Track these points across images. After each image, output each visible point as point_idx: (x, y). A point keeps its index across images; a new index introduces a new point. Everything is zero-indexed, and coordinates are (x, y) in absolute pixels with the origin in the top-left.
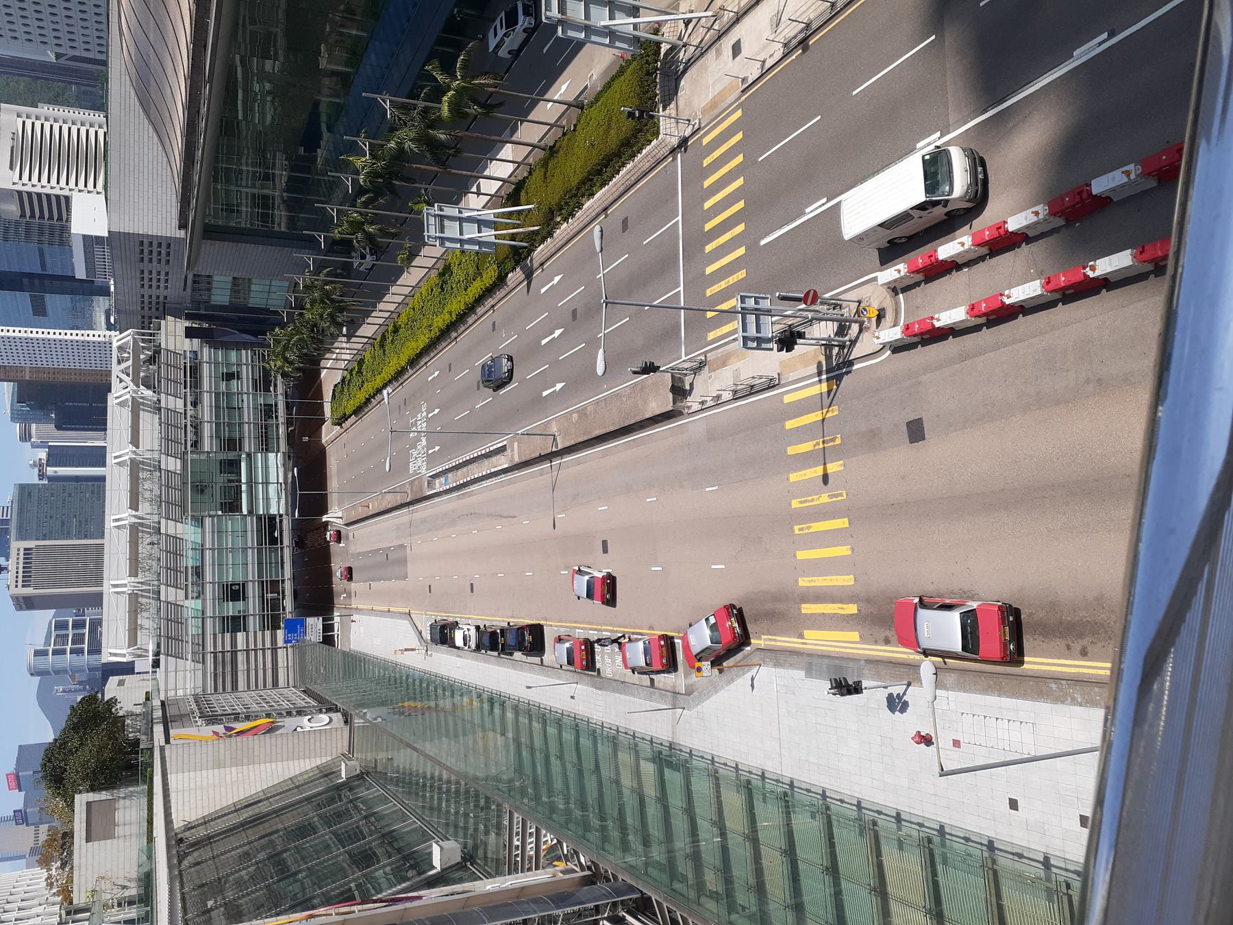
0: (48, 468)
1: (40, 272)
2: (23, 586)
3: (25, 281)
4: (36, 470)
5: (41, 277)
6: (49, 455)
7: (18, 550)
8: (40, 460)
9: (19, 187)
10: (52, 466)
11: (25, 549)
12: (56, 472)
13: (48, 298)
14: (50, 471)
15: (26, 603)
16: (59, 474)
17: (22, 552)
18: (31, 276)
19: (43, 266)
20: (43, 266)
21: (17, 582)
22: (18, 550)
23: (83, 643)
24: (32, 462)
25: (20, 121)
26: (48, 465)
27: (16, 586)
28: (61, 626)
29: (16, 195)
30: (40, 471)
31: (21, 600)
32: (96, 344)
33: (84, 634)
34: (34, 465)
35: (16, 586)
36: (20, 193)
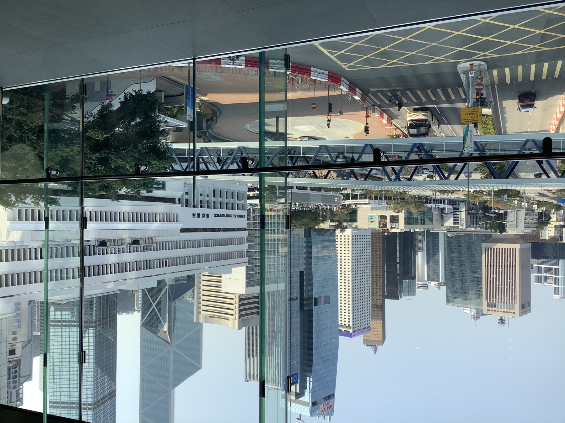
0: (440, 282)
1: (299, 301)
2: (514, 309)
3: (306, 308)
4: (441, 287)
5: (302, 299)
6: (433, 280)
7: (489, 310)
8: (435, 285)
9: (237, 316)
10: (439, 279)
11: (488, 306)
12: (442, 278)
13: (314, 296)
14: (441, 280)
15: (526, 307)
16: (444, 277)
17: (490, 308)
18: (302, 305)
19: (297, 299)
20: (297, 299)
21: (510, 313)
22: (489, 310)
23: (552, 268)
24: (437, 289)
25: (203, 313)
26: (438, 281)
27: (514, 313)
28: (539, 280)
29: (242, 318)
30: (442, 285)
31: (524, 310)
32: (354, 264)
33: (545, 268)
34: (439, 288)
35: (514, 313)
36: (240, 316)
